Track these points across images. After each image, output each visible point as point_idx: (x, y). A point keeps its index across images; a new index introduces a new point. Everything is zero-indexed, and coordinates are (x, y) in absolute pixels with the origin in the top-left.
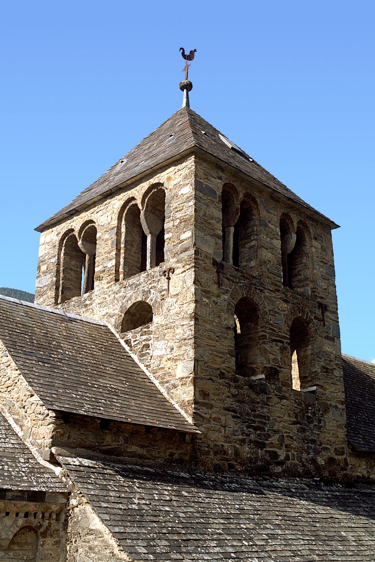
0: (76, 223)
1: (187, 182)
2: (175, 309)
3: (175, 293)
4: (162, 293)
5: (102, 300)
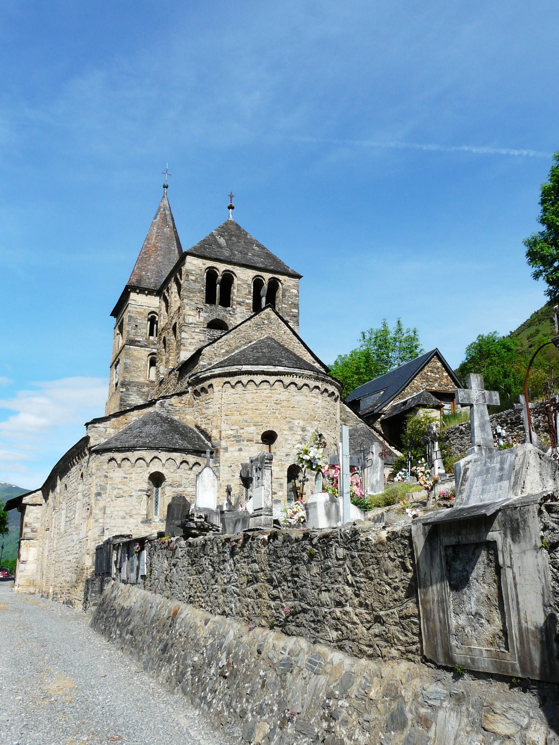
0: (222, 268)
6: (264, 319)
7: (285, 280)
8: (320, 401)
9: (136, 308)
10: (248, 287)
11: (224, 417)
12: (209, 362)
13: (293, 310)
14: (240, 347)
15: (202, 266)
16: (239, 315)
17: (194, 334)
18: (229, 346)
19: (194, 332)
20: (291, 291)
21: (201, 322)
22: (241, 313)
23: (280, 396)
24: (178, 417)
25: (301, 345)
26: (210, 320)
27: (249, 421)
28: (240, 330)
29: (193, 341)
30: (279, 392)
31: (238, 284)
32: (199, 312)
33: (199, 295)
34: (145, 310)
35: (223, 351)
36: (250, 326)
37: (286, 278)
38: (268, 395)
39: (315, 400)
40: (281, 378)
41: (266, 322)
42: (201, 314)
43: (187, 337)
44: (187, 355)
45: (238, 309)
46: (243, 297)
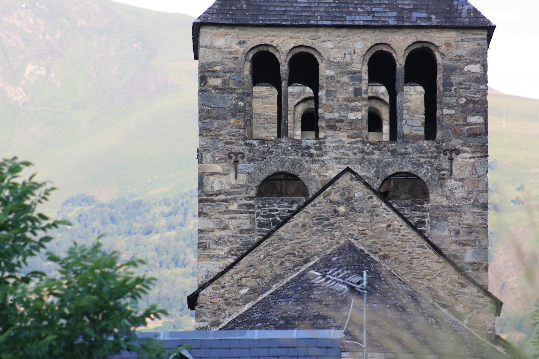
1: (477, 60)
3: (461, 177)
4: (442, 172)
5: (340, 156)
37: (452, 35)
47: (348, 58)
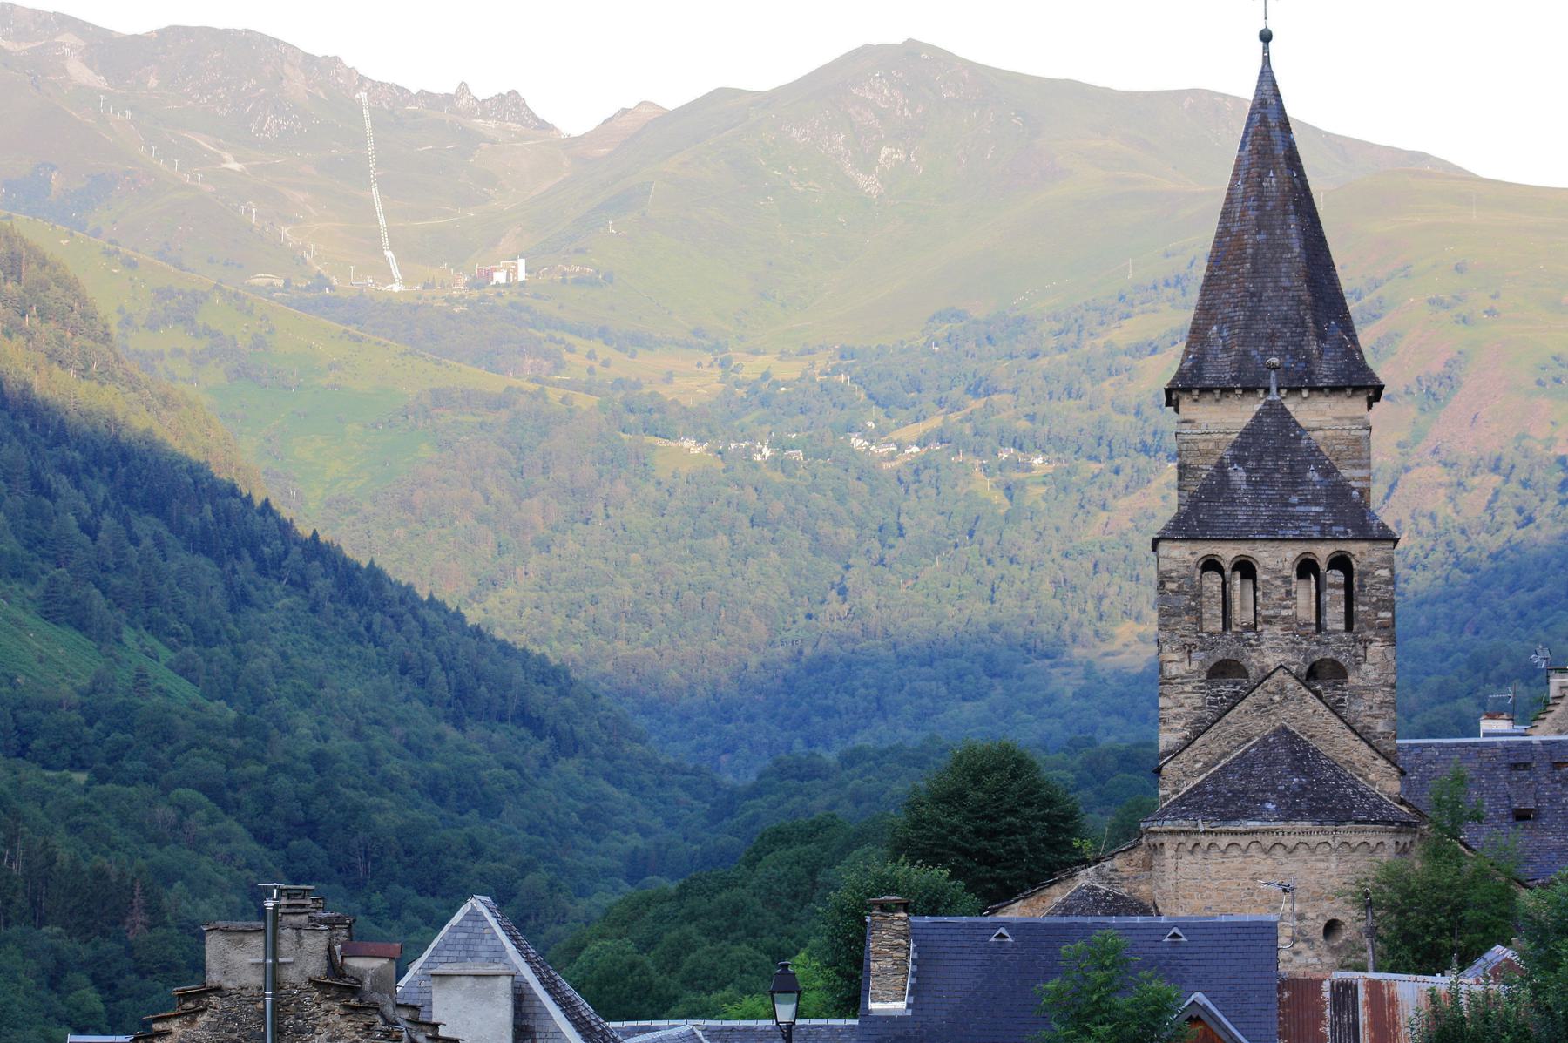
2: (1373, 675)
6: (1274, 693)
7: (1362, 553)
8: (1333, 865)
9: (1195, 442)
10: (1284, 582)
11: (1182, 900)
12: (1174, 788)
13: (1382, 614)
14: (1228, 753)
15: (1190, 557)
16: (1268, 644)
17: (1182, 696)
18: (1210, 753)
19: (1181, 693)
20: (1377, 573)
21: (1194, 672)
22: (1272, 639)
23: (1258, 868)
24: (1126, 890)
25: (1346, 730)
26: (1212, 663)
27: (1213, 908)
28: (1228, 723)
29: (1180, 710)
30: (1256, 860)
31: (1264, 581)
32: (1190, 652)
33: (1186, 618)
34: (1217, 443)
35: (1199, 765)
36: (1246, 712)
37: (1365, 546)
38: (1240, 866)
39: (1322, 865)
40: (1259, 837)
41: (1277, 698)
42: (1193, 655)
43: (1170, 705)
44: (1171, 739)
45: (1266, 632)
46: (1275, 606)
47: (1280, 565)
